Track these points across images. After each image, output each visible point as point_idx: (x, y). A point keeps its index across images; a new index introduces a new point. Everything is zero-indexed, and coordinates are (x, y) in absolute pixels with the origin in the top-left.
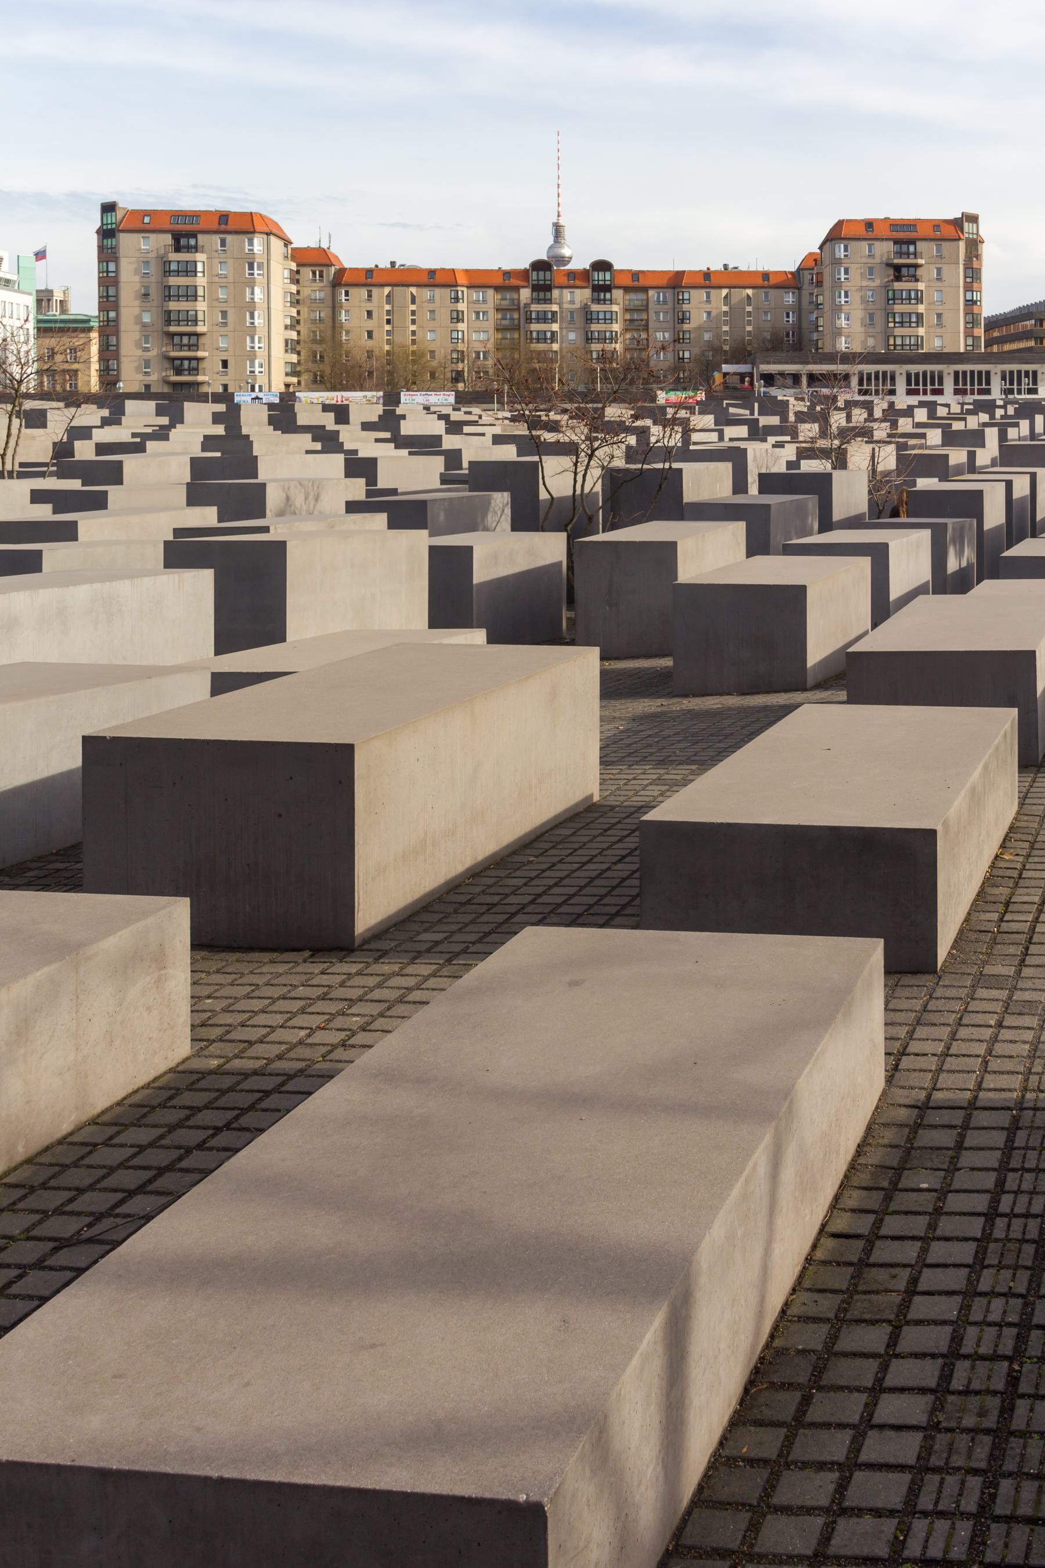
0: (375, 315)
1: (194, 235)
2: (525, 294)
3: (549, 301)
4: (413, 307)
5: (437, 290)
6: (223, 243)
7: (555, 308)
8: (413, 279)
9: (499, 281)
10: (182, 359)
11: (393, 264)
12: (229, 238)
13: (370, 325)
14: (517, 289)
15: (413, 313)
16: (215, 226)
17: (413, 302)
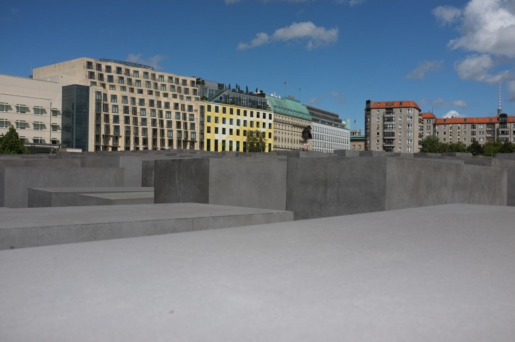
0: (447, 133)
1: (392, 109)
2: (497, 125)
3: (506, 127)
4: (459, 131)
5: (467, 125)
6: (401, 111)
7: (508, 130)
8: (459, 122)
9: (488, 121)
10: (388, 147)
11: (452, 117)
12: (402, 109)
13: (445, 136)
14: (494, 124)
15: (459, 132)
16: (398, 106)
17: (459, 129)
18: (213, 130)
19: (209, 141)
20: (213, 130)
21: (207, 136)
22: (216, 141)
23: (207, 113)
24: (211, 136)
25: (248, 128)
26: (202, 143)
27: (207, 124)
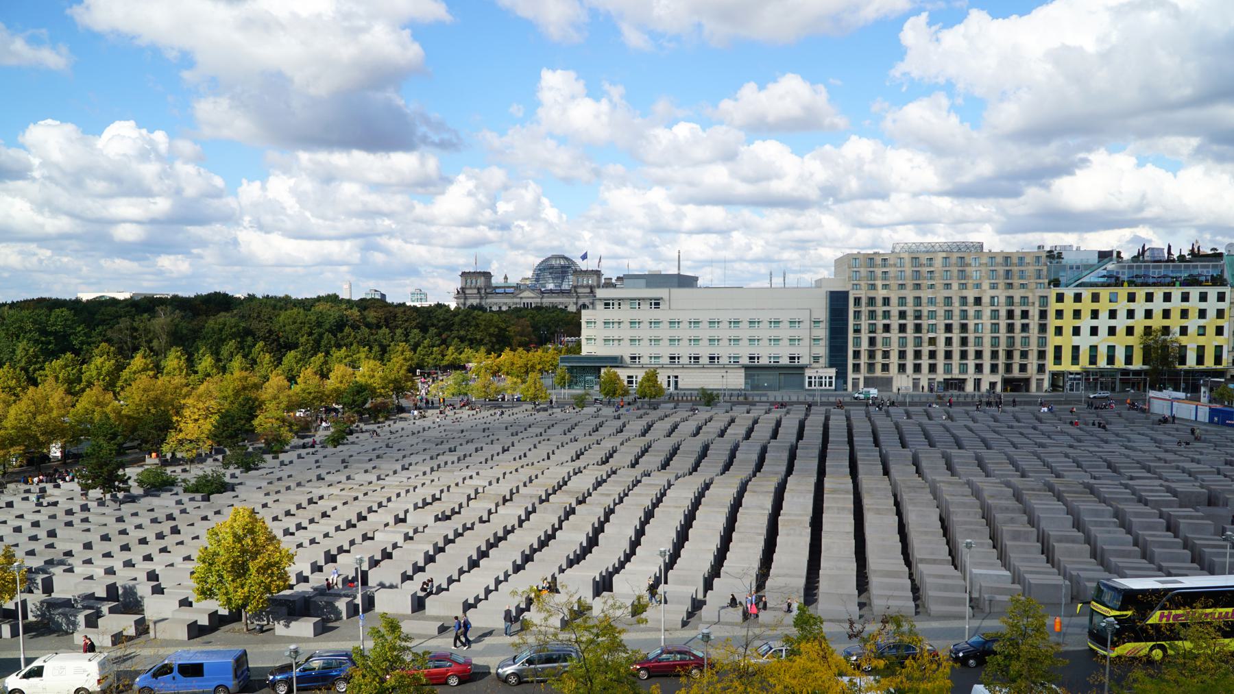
18: (1068, 331)
19: (1058, 349)
20: (1068, 331)
21: (1053, 340)
22: (1076, 349)
23: (1053, 306)
24: (1067, 341)
25: (1157, 322)
26: (1042, 355)
27: (1052, 322)
